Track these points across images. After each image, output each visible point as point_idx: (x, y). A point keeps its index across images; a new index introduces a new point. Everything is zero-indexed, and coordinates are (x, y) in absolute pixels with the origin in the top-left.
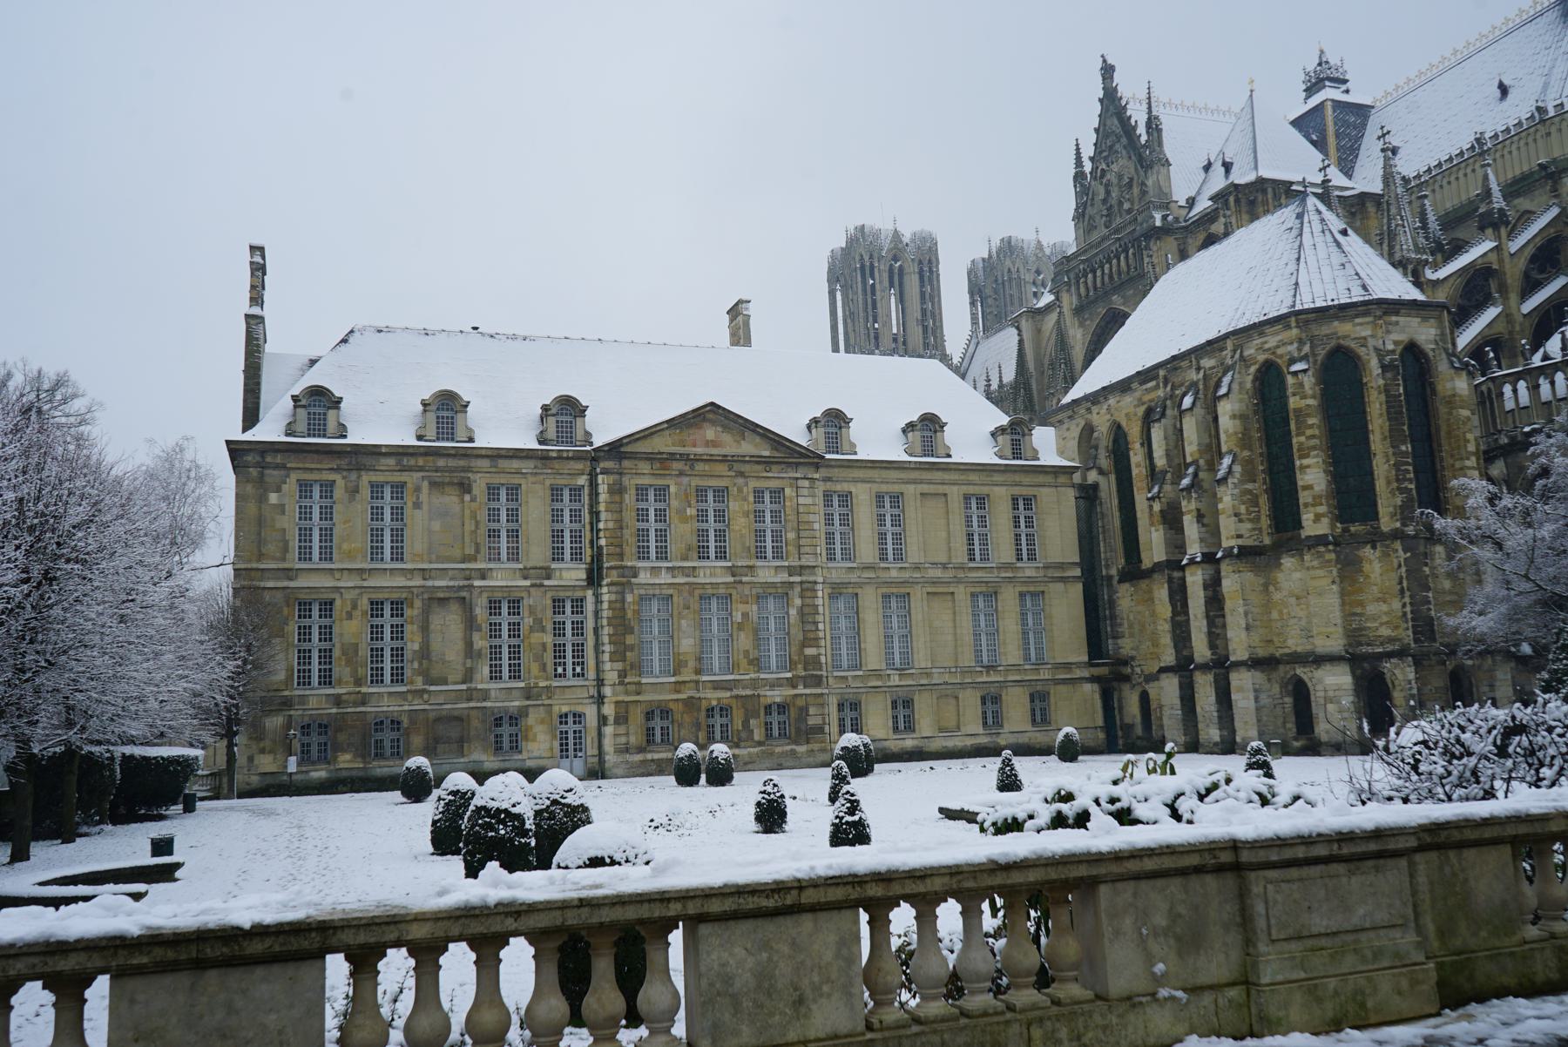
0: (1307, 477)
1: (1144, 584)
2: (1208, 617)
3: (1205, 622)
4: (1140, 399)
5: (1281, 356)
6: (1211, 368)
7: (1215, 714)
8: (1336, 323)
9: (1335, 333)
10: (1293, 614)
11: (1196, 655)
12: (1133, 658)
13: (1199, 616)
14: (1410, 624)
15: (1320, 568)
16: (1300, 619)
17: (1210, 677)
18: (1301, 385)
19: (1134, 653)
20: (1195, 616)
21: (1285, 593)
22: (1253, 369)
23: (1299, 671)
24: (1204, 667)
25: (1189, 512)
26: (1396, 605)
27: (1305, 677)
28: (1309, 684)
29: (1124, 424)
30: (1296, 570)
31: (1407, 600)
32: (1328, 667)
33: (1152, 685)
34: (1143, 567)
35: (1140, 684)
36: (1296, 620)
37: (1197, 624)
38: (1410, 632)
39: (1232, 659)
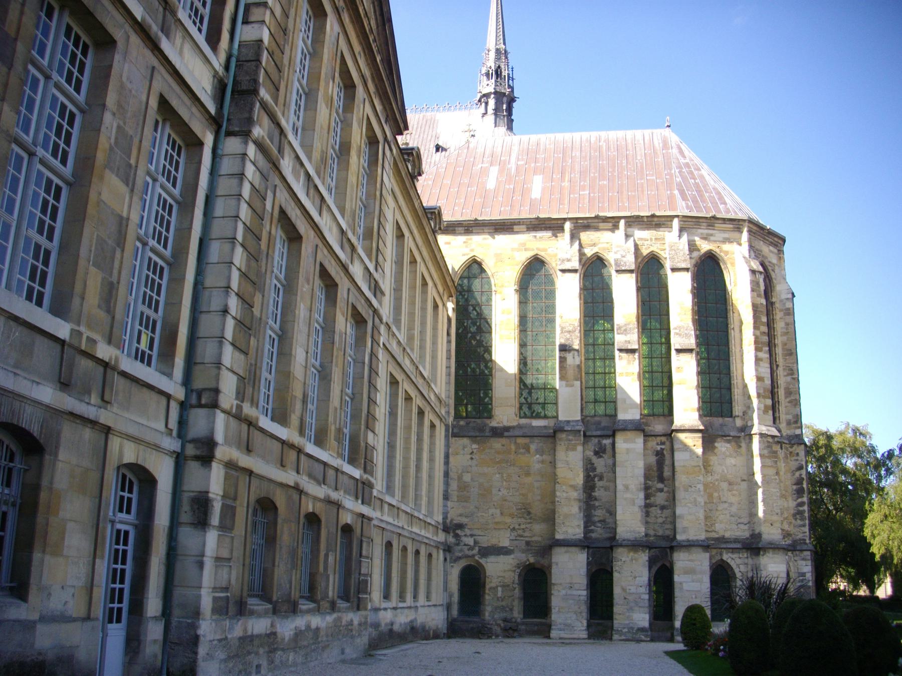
0: (760, 369)
1: (497, 444)
2: (647, 488)
3: (642, 495)
4: (524, 244)
5: (727, 253)
6: (641, 239)
7: (647, 597)
8: (762, 242)
9: (761, 251)
10: (724, 499)
11: (619, 530)
12: (460, 526)
13: (632, 487)
14: (807, 522)
15: (769, 457)
16: (731, 504)
17: (643, 557)
18: (758, 284)
19: (464, 520)
20: (627, 487)
21: (716, 477)
22: (696, 254)
23: (726, 557)
24: (635, 545)
25: (627, 374)
26: (792, 504)
27: (732, 563)
28: (736, 571)
29: (489, 266)
30: (731, 456)
31: (805, 499)
32: (770, 554)
33: (492, 559)
34: (494, 424)
35: (467, 557)
36: (726, 505)
37: (628, 495)
38: (807, 529)
39: (679, 537)
